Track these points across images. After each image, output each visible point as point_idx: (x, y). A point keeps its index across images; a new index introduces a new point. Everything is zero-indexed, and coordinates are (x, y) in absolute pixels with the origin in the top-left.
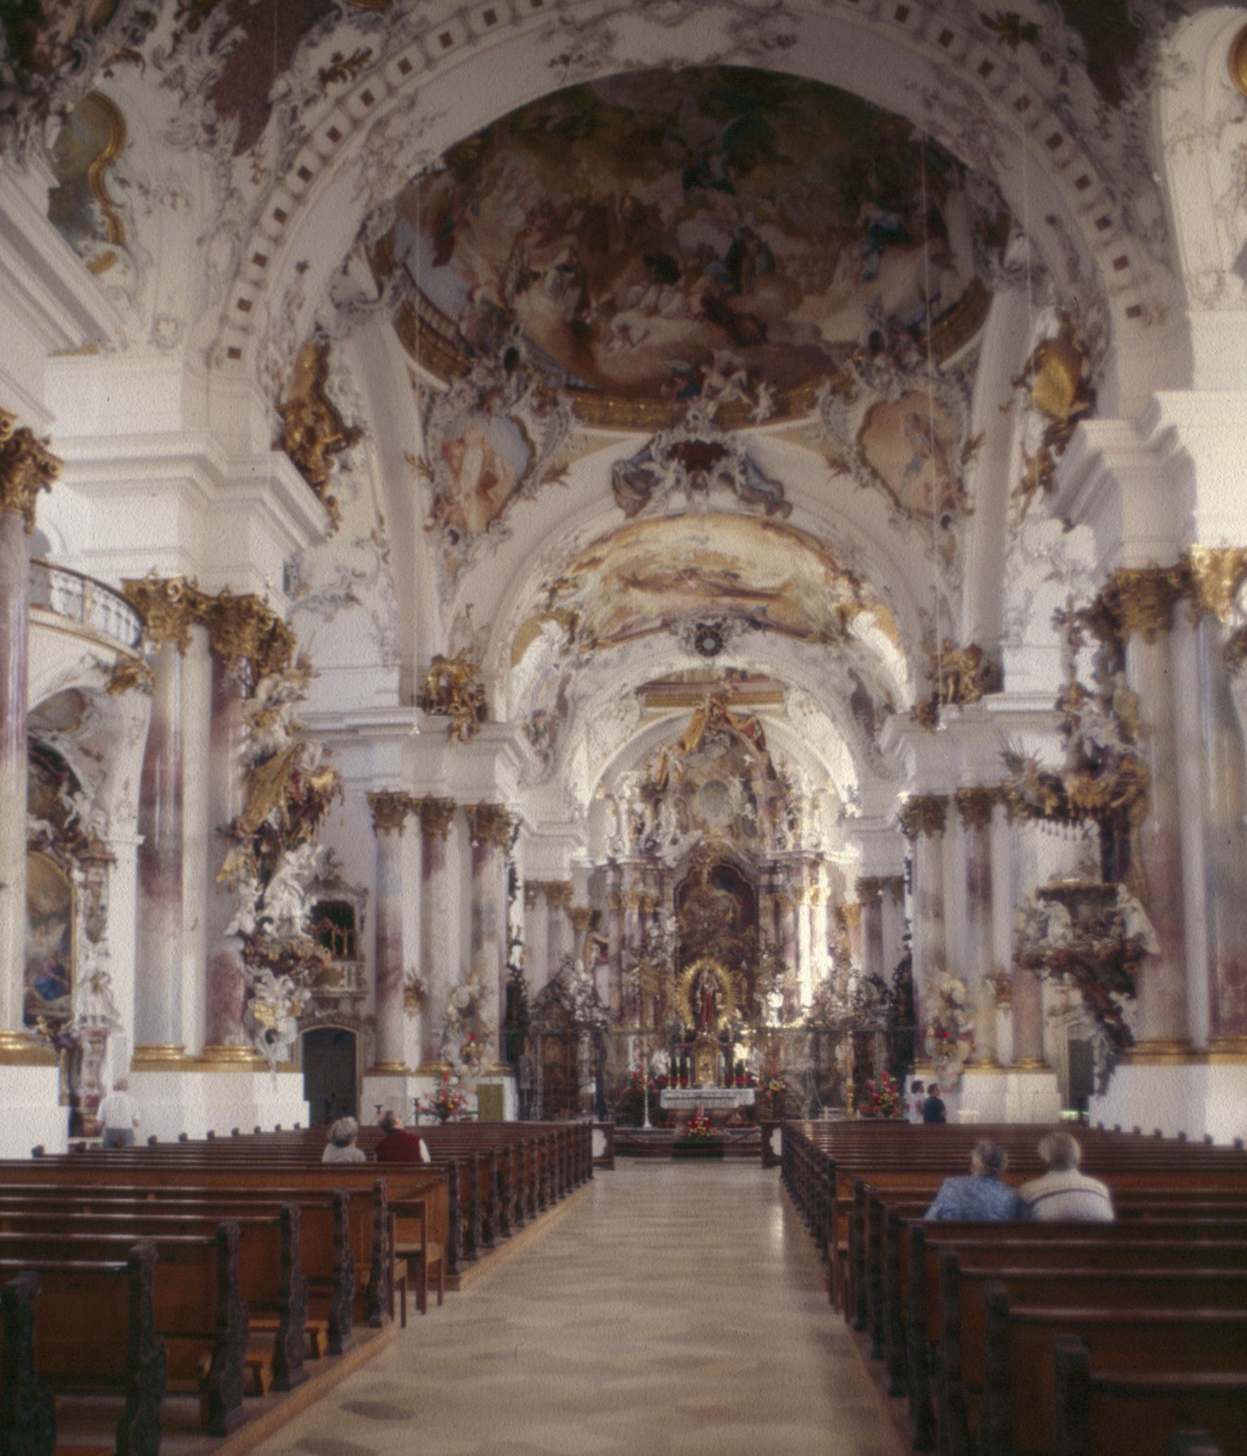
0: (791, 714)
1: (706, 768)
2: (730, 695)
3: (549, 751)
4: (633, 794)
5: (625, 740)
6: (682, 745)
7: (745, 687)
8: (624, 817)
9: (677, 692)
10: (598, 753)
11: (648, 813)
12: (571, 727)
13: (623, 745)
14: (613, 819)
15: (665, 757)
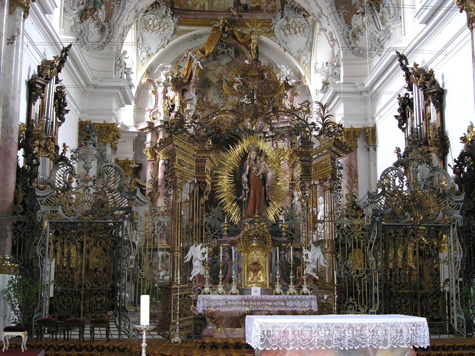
0: (276, 34)
1: (218, 71)
2: (237, 18)
3: (105, 24)
4: (168, 80)
5: (163, 46)
6: (203, 52)
7: (246, 16)
8: (161, 97)
9: (201, 17)
10: (144, 54)
11: (177, 98)
12: (124, 8)
13: (162, 50)
14: (153, 97)
15: (191, 60)
